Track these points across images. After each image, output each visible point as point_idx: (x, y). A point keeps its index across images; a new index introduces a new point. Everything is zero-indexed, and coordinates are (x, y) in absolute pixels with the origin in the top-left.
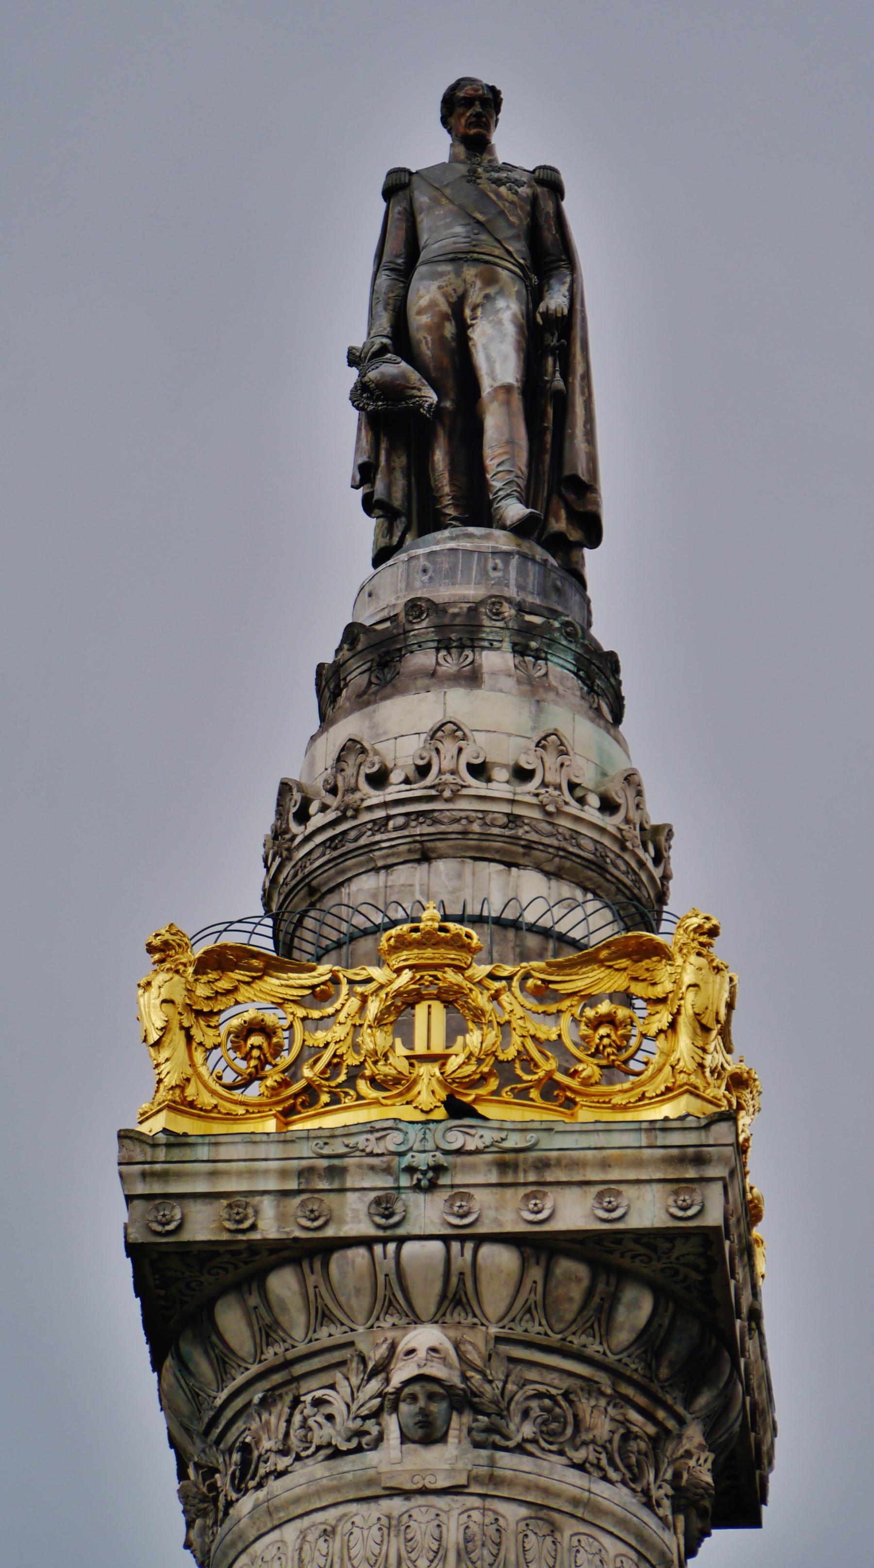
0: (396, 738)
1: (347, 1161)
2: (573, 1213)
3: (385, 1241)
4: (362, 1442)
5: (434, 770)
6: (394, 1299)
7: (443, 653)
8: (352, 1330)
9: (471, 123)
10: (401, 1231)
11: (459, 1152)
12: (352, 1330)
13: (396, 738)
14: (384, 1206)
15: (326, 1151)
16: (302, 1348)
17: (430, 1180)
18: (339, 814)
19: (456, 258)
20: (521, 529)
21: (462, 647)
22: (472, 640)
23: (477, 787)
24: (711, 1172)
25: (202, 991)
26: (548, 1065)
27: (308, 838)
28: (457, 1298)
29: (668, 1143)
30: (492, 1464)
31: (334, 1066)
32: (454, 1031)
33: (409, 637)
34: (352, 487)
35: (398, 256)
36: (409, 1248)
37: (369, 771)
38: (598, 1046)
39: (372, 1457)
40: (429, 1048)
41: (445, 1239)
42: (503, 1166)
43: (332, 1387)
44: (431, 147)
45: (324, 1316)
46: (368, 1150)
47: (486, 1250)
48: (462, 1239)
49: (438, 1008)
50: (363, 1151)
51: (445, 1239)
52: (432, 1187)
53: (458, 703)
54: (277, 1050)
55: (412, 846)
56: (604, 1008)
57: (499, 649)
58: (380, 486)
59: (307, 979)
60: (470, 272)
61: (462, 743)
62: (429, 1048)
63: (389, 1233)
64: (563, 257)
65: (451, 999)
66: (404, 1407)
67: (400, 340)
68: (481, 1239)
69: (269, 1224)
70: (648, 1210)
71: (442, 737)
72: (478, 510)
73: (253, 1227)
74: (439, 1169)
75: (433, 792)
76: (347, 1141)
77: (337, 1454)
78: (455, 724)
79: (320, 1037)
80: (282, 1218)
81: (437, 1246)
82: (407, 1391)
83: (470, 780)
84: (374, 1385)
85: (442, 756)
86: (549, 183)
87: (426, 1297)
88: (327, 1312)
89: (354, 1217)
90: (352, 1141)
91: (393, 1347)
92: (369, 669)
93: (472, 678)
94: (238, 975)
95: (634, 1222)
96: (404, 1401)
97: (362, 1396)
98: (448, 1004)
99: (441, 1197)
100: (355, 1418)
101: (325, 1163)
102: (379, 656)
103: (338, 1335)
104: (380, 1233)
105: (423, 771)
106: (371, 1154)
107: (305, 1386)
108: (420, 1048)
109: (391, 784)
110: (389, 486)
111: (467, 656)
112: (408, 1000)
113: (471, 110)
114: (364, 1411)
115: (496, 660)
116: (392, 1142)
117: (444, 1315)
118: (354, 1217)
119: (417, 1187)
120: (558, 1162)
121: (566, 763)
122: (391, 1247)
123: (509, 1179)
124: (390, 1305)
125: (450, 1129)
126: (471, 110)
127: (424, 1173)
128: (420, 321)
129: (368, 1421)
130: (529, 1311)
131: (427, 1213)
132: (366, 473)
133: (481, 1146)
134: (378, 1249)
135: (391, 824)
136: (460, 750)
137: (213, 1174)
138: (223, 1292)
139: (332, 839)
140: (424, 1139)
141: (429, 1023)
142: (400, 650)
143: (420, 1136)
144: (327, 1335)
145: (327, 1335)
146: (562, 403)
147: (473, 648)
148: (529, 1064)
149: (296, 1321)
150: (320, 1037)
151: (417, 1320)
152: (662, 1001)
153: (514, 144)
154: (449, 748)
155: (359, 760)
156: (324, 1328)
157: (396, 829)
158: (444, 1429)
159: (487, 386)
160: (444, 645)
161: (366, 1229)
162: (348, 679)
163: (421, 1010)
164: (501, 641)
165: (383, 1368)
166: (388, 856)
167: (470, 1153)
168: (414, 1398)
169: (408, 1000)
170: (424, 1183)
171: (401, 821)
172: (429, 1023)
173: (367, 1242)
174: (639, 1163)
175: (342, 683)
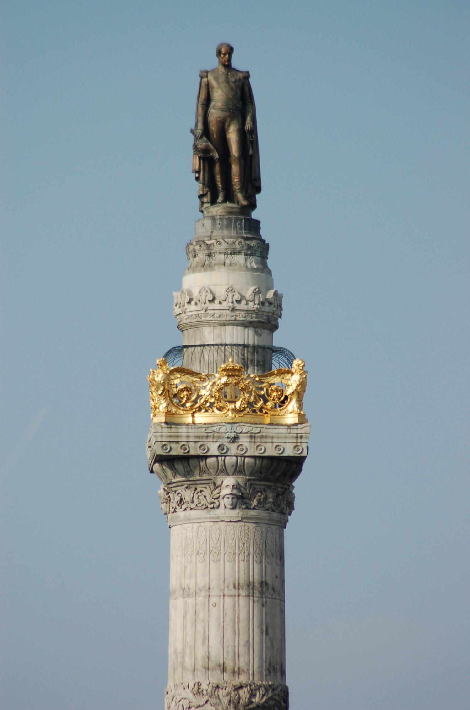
3: (221, 456)
6: (224, 471)
14: (221, 447)
31: (206, 401)
41: (237, 457)
47: (247, 459)
67: (206, 132)
86: (247, 76)
87: (230, 470)
89: (214, 449)
107: (198, 486)
113: (226, 53)
114: (214, 497)
118: (214, 449)
122: (223, 458)
126: (226, 53)
131: (233, 449)
134: (220, 458)
161: (217, 453)
173: (217, 456)
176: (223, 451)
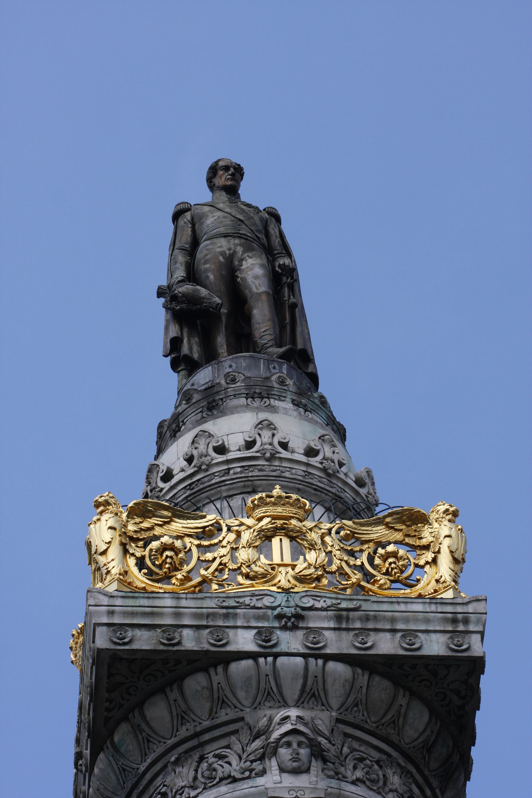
0: (228, 435)
1: (238, 611)
2: (386, 645)
3: (265, 656)
4: (250, 774)
5: (258, 443)
6: (271, 693)
7: (250, 400)
8: (242, 710)
9: (228, 179)
10: (275, 650)
11: (311, 609)
12: (242, 710)
13: (228, 435)
14: (264, 636)
15: (225, 604)
16: (207, 724)
17: (293, 621)
18: (196, 469)
21: (262, 398)
22: (268, 394)
23: (284, 454)
24: (471, 628)
25: (131, 527)
26: (356, 577)
27: (172, 488)
28: (311, 693)
29: (444, 610)
30: (340, 785)
31: (220, 570)
32: (298, 552)
33: (227, 392)
34: (163, 356)
35: (187, 244)
36: (281, 660)
37: (215, 445)
38: (388, 569)
39: (261, 781)
40: (282, 560)
41: (304, 656)
42: (339, 619)
43: (228, 747)
45: (223, 703)
46: (252, 605)
47: (331, 665)
48: (316, 657)
49: (286, 542)
50: (249, 605)
51: (304, 656)
52: (295, 628)
54: (183, 562)
55: (246, 483)
56: (391, 548)
57: (284, 401)
58: (185, 350)
59: (201, 523)
61: (275, 432)
62: (282, 560)
63: (268, 650)
64: (284, 252)
65: (295, 536)
66: (282, 751)
68: (328, 658)
69: (189, 641)
70: (435, 646)
71: (262, 428)
73: (179, 643)
74: (299, 617)
75: (258, 454)
76: (237, 600)
77: (235, 780)
78: (269, 421)
79: (209, 556)
80: (198, 640)
81: (299, 660)
82: (284, 740)
83: (280, 449)
84: (258, 743)
85: (263, 437)
87: (292, 691)
88: (226, 699)
90: (241, 600)
91: (271, 720)
92: (201, 412)
93: (273, 409)
94: (154, 520)
95: (426, 651)
96: (282, 747)
97: (250, 749)
98: (292, 539)
99: (300, 634)
100: (245, 762)
101: (224, 611)
102: (208, 403)
103: (232, 714)
104: (262, 650)
105: (250, 445)
106: (254, 608)
107: (208, 748)
108: (277, 559)
109: (230, 451)
110: (191, 349)
111: (266, 402)
112: (266, 536)
113: (226, 178)
114: (252, 757)
116: (267, 601)
117: (303, 703)
118: (244, 640)
119: (284, 628)
120: (375, 618)
121: (336, 451)
122: (270, 659)
123: (344, 626)
124: (269, 695)
125: (303, 597)
126: (226, 178)
127: (289, 618)
129: (254, 763)
130: (357, 705)
131: (291, 641)
133: (325, 605)
134: (261, 660)
135: (232, 472)
136: (273, 435)
137: (152, 614)
138: (152, 694)
139: (190, 485)
140: (287, 601)
141: (281, 548)
142: (222, 399)
143: (285, 599)
144: (224, 715)
145: (224, 715)
147: (269, 398)
148: (346, 576)
149: (201, 707)
150: (209, 556)
151: (286, 705)
152: (427, 547)
154: (266, 435)
155: (208, 441)
156: (223, 710)
157: (234, 474)
158: (308, 766)
161: (251, 647)
162: (185, 421)
163: (276, 541)
164: (285, 397)
165: (266, 732)
166: (230, 489)
167: (317, 609)
168: (289, 744)
169: (266, 536)
170: (289, 624)
171: (239, 470)
172: (281, 548)
173: (253, 656)
174: (427, 621)
175: (181, 424)
176: (268, 649)
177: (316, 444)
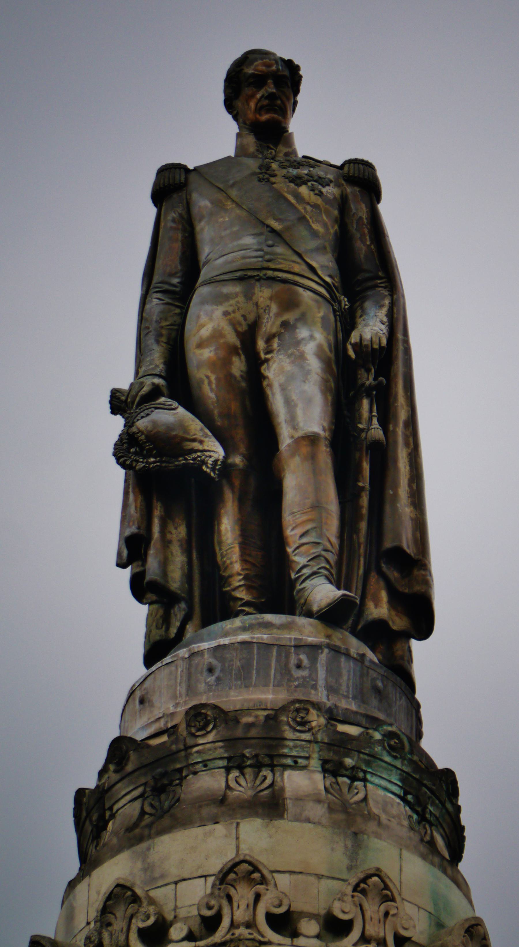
0: (176, 883)
5: (226, 922)
7: (235, 773)
9: (262, 107)
13: (176, 883)
19: (246, 277)
20: (333, 616)
21: (258, 766)
22: (271, 757)
33: (191, 754)
34: (118, 565)
35: (172, 275)
37: (141, 925)
44: (212, 138)
53: (254, 837)
57: (305, 767)
58: (153, 563)
60: (263, 294)
61: (261, 888)
64: (380, 274)
67: (177, 381)
71: (235, 880)
72: (277, 591)
78: (250, 863)
85: (235, 905)
86: (361, 180)
92: (141, 796)
93: (272, 806)
102: (154, 778)
105: (211, 924)
109: (171, 941)
110: (164, 564)
111: (265, 778)
113: (262, 90)
115: (301, 782)
121: (392, 912)
126: (262, 90)
128: (201, 357)
132: (134, 549)
136: (258, 897)
142: (180, 770)
146: (382, 456)
147: (272, 767)
153: (317, 132)
154: (243, 894)
155: (130, 911)
159: (286, 437)
160: (235, 764)
162: (116, 808)
164: (307, 758)
175: (108, 814)
177: (343, 910)
